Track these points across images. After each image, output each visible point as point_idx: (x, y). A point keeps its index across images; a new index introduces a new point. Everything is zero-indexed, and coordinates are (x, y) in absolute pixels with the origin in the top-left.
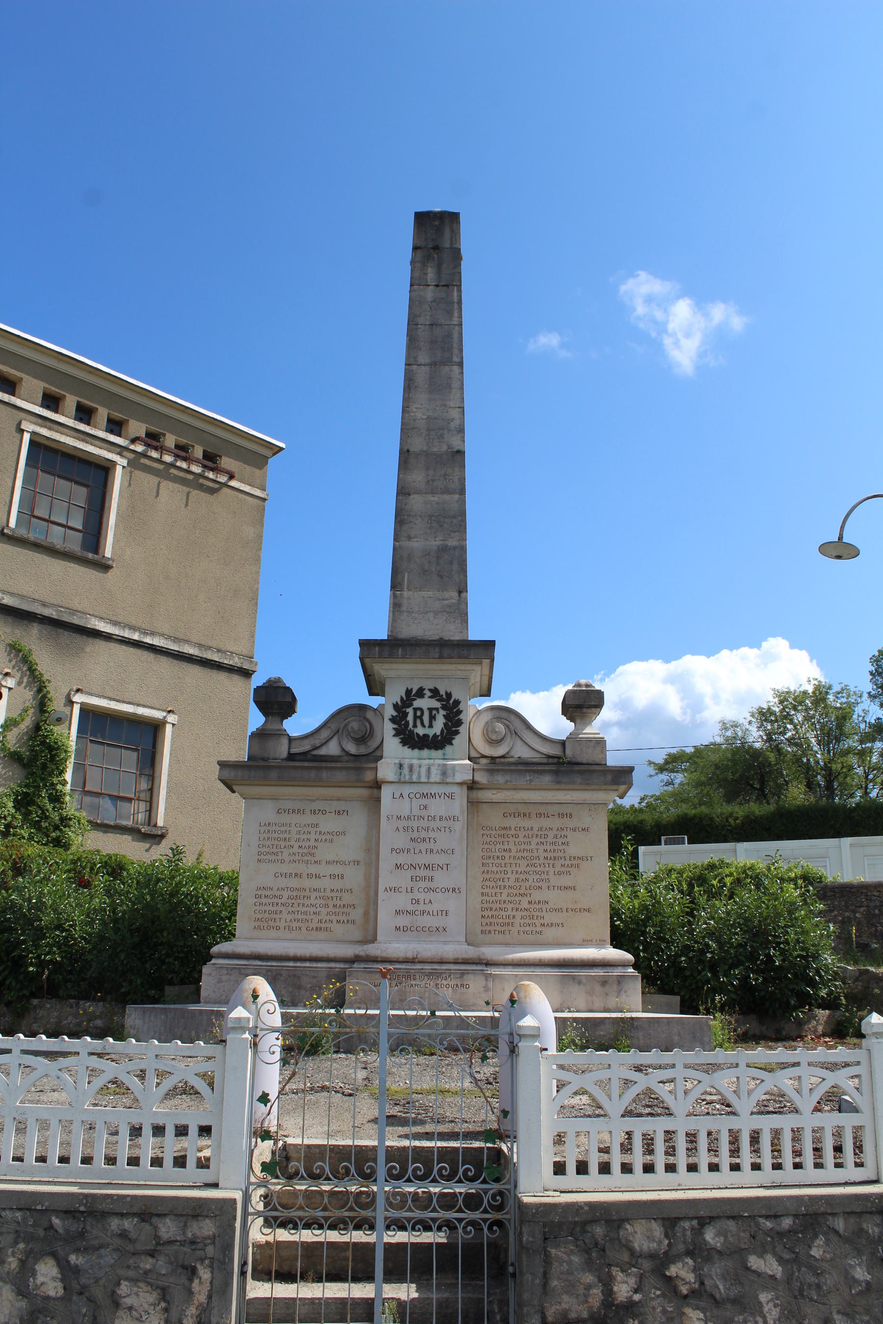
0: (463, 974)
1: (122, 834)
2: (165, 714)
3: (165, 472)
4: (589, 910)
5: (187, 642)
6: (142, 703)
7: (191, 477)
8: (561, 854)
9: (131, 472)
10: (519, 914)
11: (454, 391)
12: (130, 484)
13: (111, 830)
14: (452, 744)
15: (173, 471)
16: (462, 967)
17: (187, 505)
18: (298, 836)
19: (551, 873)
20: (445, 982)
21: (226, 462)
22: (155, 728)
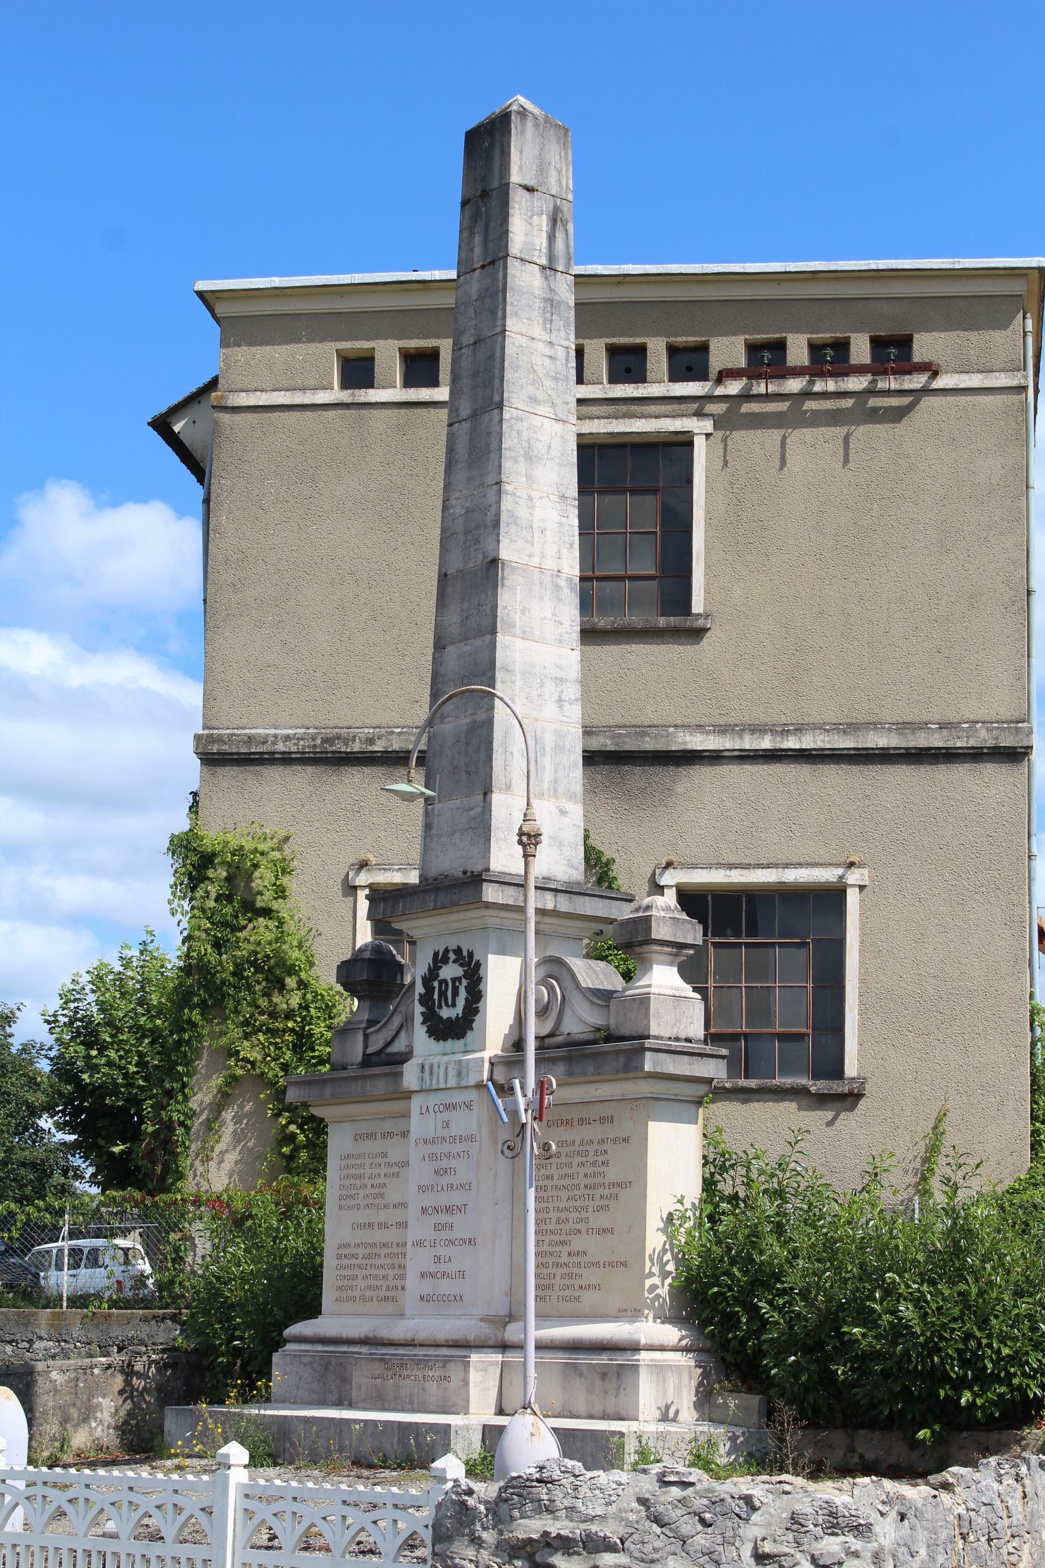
0: (446, 1361)
1: (777, 1101)
2: (840, 871)
3: (795, 415)
4: (624, 1264)
5: (874, 726)
6: (796, 860)
7: (848, 403)
8: (600, 1180)
9: (724, 440)
10: (559, 1271)
11: (492, 455)
12: (726, 463)
13: (757, 1097)
14: (472, 1029)
15: (810, 405)
16: (445, 1351)
17: (846, 461)
18: (372, 1171)
19: (590, 1209)
20: (431, 1373)
21: (925, 346)
22: (832, 898)
